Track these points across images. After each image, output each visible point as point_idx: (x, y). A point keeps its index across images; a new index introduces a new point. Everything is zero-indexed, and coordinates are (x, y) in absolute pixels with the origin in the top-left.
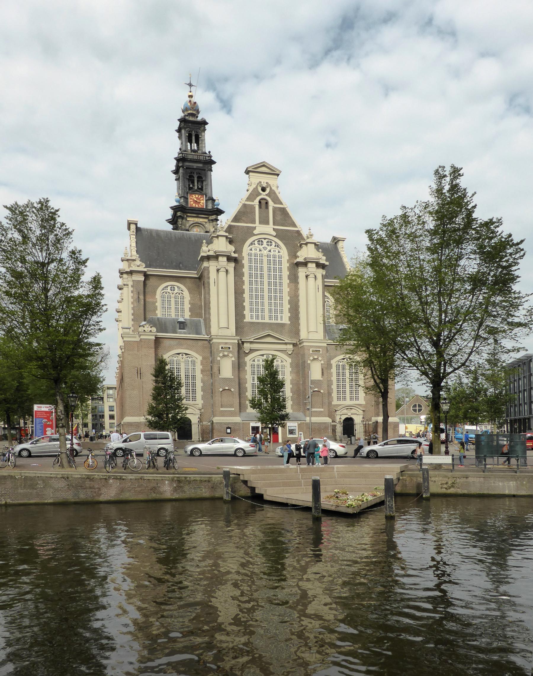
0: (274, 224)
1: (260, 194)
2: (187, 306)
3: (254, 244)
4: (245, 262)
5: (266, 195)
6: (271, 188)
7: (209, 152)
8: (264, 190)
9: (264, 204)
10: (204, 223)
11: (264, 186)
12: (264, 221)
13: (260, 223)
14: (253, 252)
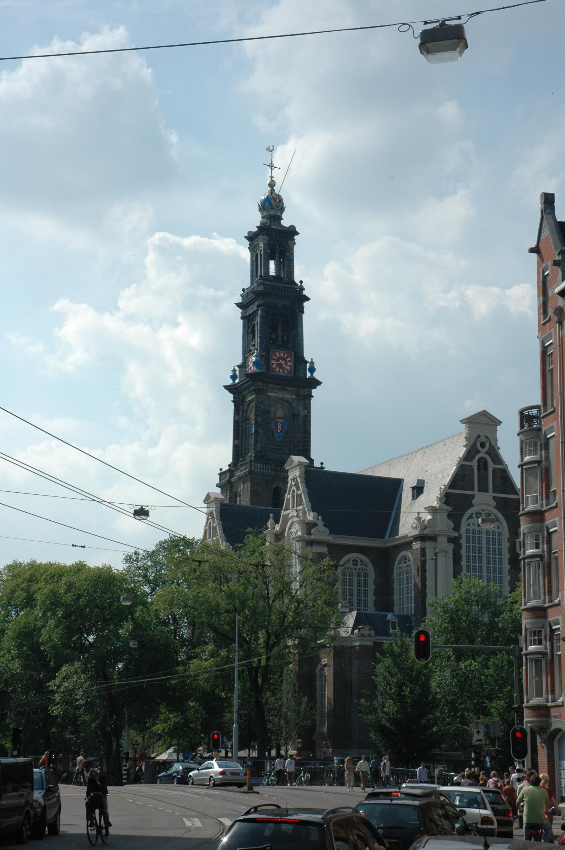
0: (494, 492)
1: (478, 452)
2: (371, 587)
3: (472, 518)
4: (463, 541)
5: (486, 453)
6: (490, 444)
7: (301, 282)
8: (483, 445)
9: (483, 464)
10: (291, 400)
11: (483, 441)
12: (483, 488)
13: (479, 491)
14: (471, 528)
